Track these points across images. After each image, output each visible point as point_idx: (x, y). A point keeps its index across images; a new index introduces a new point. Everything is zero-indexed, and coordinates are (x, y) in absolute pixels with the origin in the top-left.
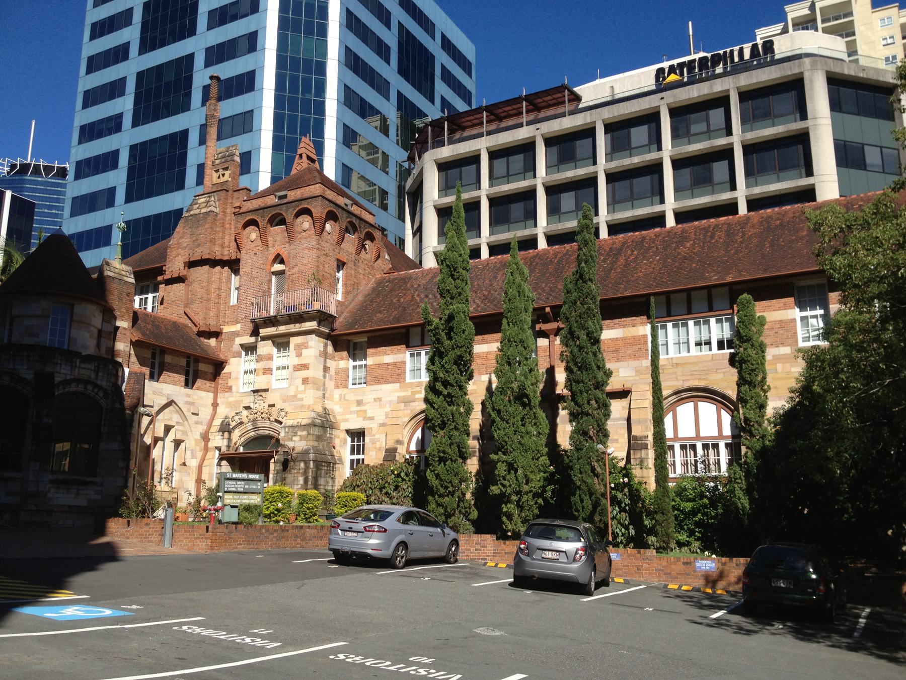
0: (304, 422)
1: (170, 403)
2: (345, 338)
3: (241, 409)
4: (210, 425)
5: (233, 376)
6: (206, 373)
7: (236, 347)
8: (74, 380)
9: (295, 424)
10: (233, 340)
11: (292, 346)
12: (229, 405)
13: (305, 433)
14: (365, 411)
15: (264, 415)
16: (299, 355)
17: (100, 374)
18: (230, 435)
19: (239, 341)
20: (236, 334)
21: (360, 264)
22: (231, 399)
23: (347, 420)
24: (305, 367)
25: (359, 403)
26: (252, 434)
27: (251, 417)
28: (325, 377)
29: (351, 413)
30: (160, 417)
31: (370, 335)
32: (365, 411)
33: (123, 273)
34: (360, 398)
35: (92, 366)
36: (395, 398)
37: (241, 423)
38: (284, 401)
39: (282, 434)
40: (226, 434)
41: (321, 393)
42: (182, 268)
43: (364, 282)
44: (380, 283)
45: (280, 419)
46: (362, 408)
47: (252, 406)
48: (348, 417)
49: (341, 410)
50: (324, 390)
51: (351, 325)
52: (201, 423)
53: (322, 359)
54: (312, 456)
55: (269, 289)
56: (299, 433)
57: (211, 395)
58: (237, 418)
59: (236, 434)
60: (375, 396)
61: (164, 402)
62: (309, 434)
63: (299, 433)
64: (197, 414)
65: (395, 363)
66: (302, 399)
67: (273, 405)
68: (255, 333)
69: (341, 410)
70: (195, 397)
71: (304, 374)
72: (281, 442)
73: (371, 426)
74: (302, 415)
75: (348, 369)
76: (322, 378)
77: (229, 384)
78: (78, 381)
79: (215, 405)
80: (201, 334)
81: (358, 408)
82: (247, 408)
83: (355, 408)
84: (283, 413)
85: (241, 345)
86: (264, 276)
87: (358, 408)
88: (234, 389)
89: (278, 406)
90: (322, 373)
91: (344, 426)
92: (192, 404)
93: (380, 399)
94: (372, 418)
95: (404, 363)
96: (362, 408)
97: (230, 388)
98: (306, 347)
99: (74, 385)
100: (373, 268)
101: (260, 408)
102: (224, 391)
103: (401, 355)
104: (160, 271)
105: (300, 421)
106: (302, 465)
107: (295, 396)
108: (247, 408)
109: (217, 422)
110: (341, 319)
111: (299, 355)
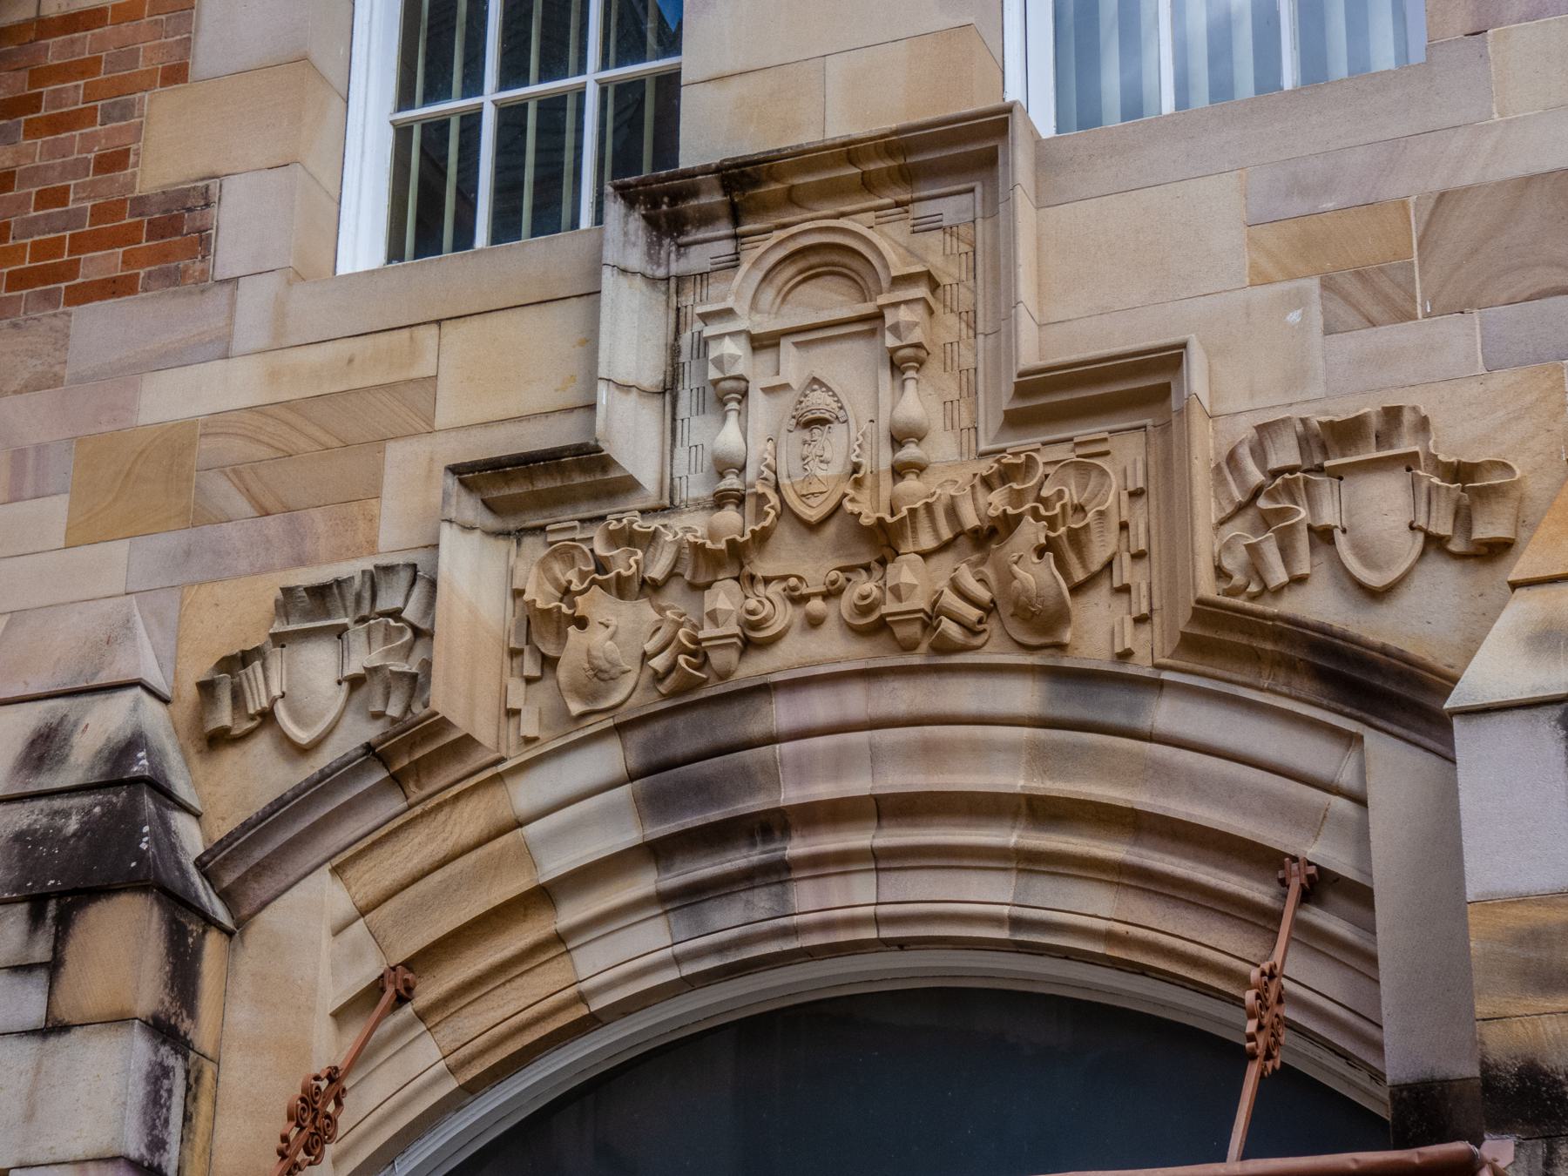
3: (408, 498)
15: (915, 579)
18: (183, 975)
26: (627, 953)
27: (619, 633)
37: (412, 753)
38: (1368, 291)
40: (120, 946)
45: (1321, 605)
47: (632, 437)
58: (311, 682)
67: (1141, 384)
77: (158, 169)
84: (1380, 511)
88: (241, 231)
89: (1238, 392)
97: (171, 237)
101: (818, 472)
108: (542, 484)
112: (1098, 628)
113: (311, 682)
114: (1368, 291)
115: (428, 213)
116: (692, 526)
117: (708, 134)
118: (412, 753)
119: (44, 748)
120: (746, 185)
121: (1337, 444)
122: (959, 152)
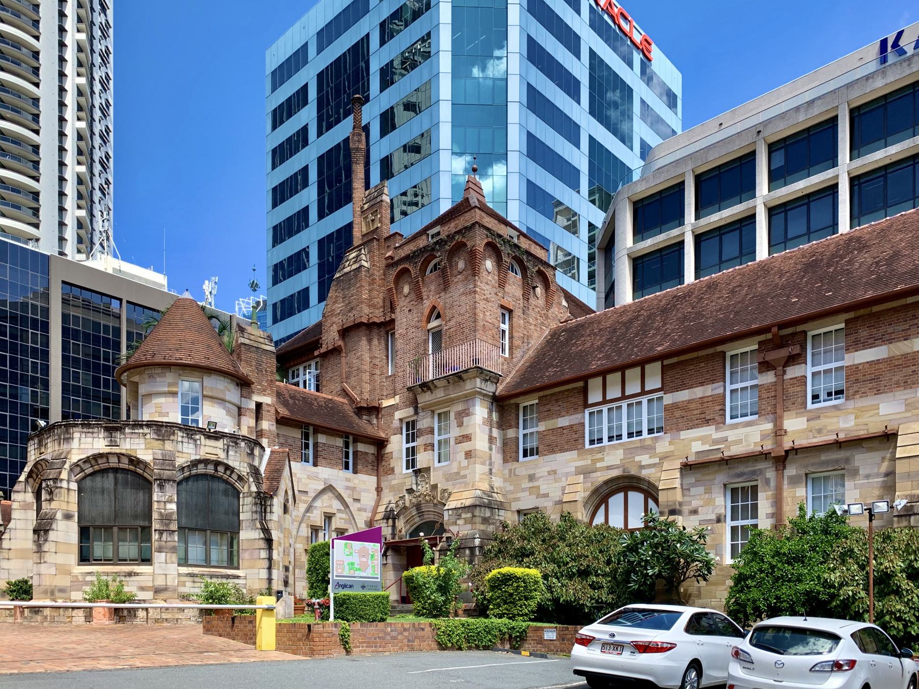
0: (468, 503)
1: (329, 488)
2: (513, 401)
4: (375, 512)
5: (395, 455)
6: (367, 453)
7: (396, 423)
8: (200, 461)
9: (459, 506)
10: (392, 415)
11: (452, 415)
12: (393, 488)
13: (469, 515)
14: (538, 487)
16: (460, 425)
17: (230, 453)
18: (394, 523)
19: (398, 415)
20: (394, 408)
21: (530, 312)
22: (394, 482)
23: (518, 499)
24: (467, 438)
25: (531, 478)
28: (491, 449)
29: (523, 490)
30: (318, 503)
31: (541, 394)
32: (538, 487)
33: (262, 340)
34: (531, 472)
35: (220, 444)
36: (574, 469)
38: (447, 480)
39: (446, 518)
41: (487, 468)
42: (337, 338)
43: (536, 334)
44: (554, 334)
46: (535, 484)
47: (414, 487)
48: (519, 495)
49: (512, 488)
50: (490, 464)
51: (518, 384)
52: (365, 510)
53: (487, 428)
54: (477, 542)
55: (426, 350)
56: (463, 516)
57: (374, 479)
59: (400, 524)
60: (549, 469)
61: (321, 487)
62: (474, 516)
63: (463, 516)
64: (358, 500)
65: (571, 426)
66: (465, 477)
67: (434, 487)
68: (415, 404)
69: (512, 488)
70: (356, 481)
71: (466, 446)
72: (446, 527)
73: (546, 504)
74: (466, 494)
75: (517, 438)
76: (487, 450)
77: (391, 466)
78: (206, 462)
79: (379, 490)
80: (360, 411)
81: (531, 485)
82: (410, 491)
83: (526, 484)
85: (401, 420)
86: (421, 335)
87: (531, 485)
90: (487, 445)
91: (516, 506)
92: (353, 489)
93: (555, 472)
94: (546, 495)
95: (583, 424)
96: (535, 484)
97: (393, 470)
98: (468, 415)
99: (201, 466)
100: (547, 318)
102: (386, 473)
103: (579, 416)
104: (317, 344)
105: (464, 501)
106: (467, 552)
107: (458, 473)
108: (410, 491)
109: (382, 509)
110: (508, 379)
111: (460, 425)
112: (435, 502)
113: (401, 502)
114: (447, 480)
115: (408, 468)
116: (418, 494)
117: (419, 466)
118: (405, 508)
119: (387, 507)
120: (420, 471)
121: (444, 491)
122: (428, 469)
